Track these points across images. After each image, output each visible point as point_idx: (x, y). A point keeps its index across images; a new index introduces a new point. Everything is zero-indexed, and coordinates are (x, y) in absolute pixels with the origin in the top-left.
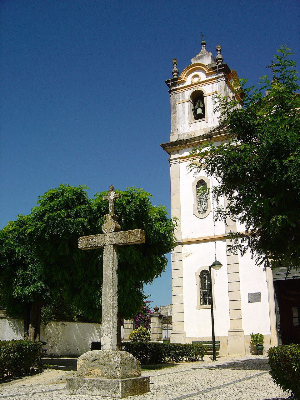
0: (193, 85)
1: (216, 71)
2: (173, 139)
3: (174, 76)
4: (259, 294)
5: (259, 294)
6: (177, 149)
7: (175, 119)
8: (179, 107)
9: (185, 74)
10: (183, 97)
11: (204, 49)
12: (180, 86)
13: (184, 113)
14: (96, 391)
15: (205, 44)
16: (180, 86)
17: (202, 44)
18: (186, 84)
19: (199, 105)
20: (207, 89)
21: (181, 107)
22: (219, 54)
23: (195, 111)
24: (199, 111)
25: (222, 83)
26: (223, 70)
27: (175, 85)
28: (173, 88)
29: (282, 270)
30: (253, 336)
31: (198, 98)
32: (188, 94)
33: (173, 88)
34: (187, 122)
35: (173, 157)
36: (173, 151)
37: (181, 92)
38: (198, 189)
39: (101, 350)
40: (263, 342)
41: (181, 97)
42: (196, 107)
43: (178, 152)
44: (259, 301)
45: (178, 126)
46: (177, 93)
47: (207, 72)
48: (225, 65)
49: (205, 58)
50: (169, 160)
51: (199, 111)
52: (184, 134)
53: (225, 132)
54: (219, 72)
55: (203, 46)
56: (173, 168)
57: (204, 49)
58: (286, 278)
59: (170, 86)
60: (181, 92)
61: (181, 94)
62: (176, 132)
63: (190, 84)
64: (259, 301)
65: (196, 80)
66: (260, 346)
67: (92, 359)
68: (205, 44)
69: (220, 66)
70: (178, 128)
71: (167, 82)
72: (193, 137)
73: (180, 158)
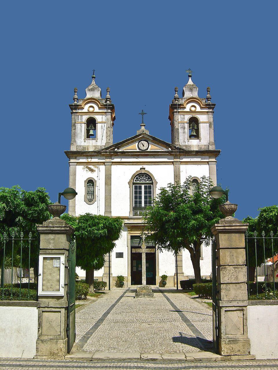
0: (89, 112)
1: (106, 108)
2: (73, 149)
3: (75, 101)
4: (123, 253)
5: (123, 253)
6: (75, 156)
7: (75, 134)
8: (78, 126)
9: (84, 103)
10: (82, 119)
11: (93, 82)
12: (80, 111)
13: (81, 131)
14: (146, 296)
15: (94, 78)
16: (80, 111)
17: (93, 78)
18: (83, 111)
19: (91, 127)
20: (99, 118)
21: (80, 126)
22: (108, 95)
23: (88, 131)
24: (91, 132)
25: (109, 116)
26: (109, 107)
27: (76, 109)
28: (74, 111)
29: (137, 241)
30: (118, 277)
31: (91, 123)
32: (85, 118)
33: (74, 111)
34: (83, 138)
35: (72, 161)
36: (72, 157)
37: (80, 115)
38: (88, 185)
39: (142, 285)
40: (124, 281)
41: (79, 119)
42: (89, 128)
43: (76, 158)
44: (122, 257)
45: (76, 139)
46: (77, 115)
47: (100, 106)
48: (113, 105)
49: (96, 91)
50: (69, 163)
51: (91, 132)
52: (80, 146)
53: (110, 152)
54: (109, 108)
55: (93, 79)
56: (71, 168)
57: (93, 82)
58: (138, 245)
59: (72, 109)
60: (80, 115)
61: (80, 117)
62: (74, 144)
63: (87, 111)
64: (122, 257)
65: (91, 109)
66: (122, 283)
67: (142, 287)
68: (94, 78)
69: (109, 105)
70: (76, 141)
71: (70, 106)
72: (87, 151)
73: (77, 163)
